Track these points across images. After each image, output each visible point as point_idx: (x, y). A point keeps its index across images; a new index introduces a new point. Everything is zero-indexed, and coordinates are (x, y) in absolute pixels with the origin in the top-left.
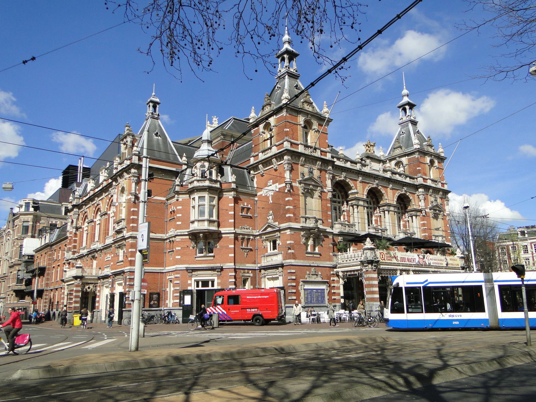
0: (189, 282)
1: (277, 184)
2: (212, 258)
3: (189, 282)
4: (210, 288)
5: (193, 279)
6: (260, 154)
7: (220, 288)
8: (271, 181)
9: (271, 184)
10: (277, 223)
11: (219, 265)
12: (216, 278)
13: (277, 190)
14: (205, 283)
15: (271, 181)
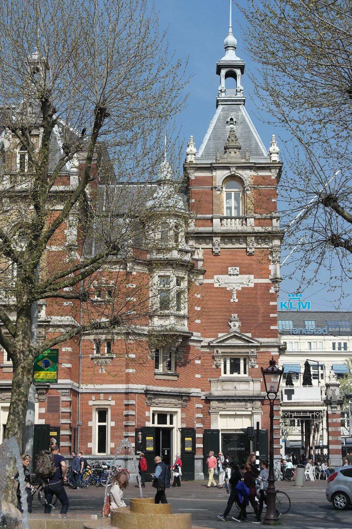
0: (147, 414)
1: (252, 277)
2: (175, 378)
3: (147, 414)
4: (168, 425)
5: (152, 409)
6: (216, 221)
7: (184, 426)
8: (238, 268)
9: (236, 272)
10: (249, 335)
11: (184, 390)
12: (179, 410)
13: (252, 285)
14: (162, 418)
15: (238, 268)
